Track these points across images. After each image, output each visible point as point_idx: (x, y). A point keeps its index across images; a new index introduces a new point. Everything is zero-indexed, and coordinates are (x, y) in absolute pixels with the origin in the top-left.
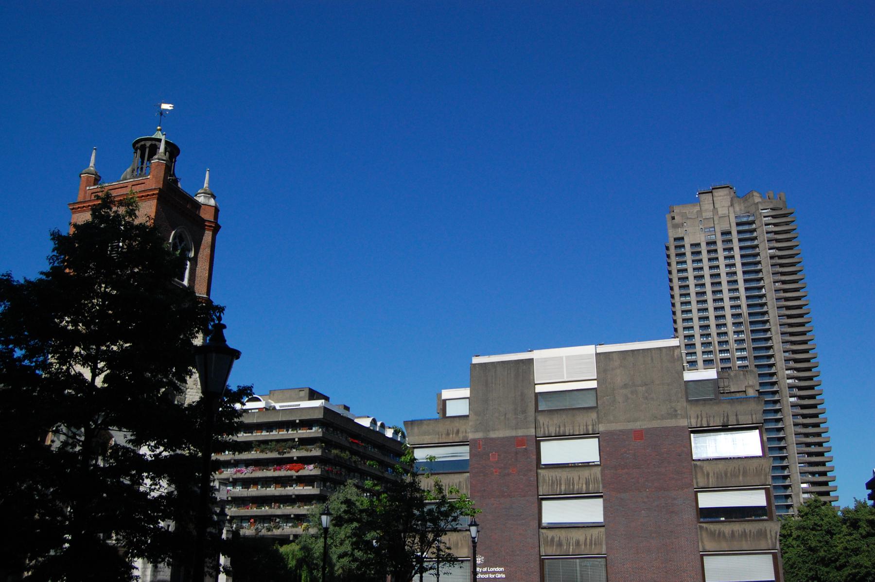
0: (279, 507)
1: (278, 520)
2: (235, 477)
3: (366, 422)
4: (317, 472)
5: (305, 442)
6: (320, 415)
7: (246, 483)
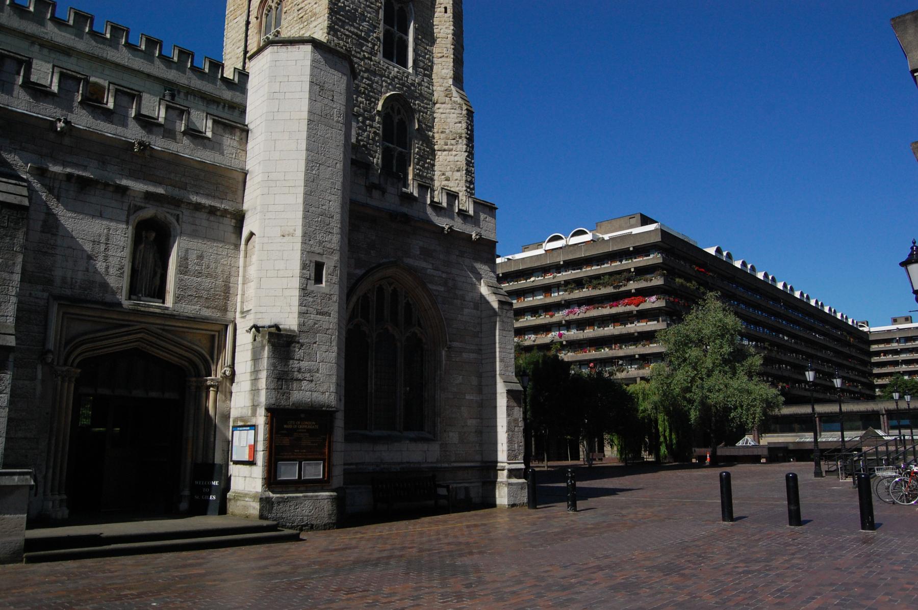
0: (621, 348)
1: (620, 362)
2: (567, 318)
3: (712, 251)
4: (661, 304)
5: (642, 272)
6: (658, 238)
7: (581, 324)
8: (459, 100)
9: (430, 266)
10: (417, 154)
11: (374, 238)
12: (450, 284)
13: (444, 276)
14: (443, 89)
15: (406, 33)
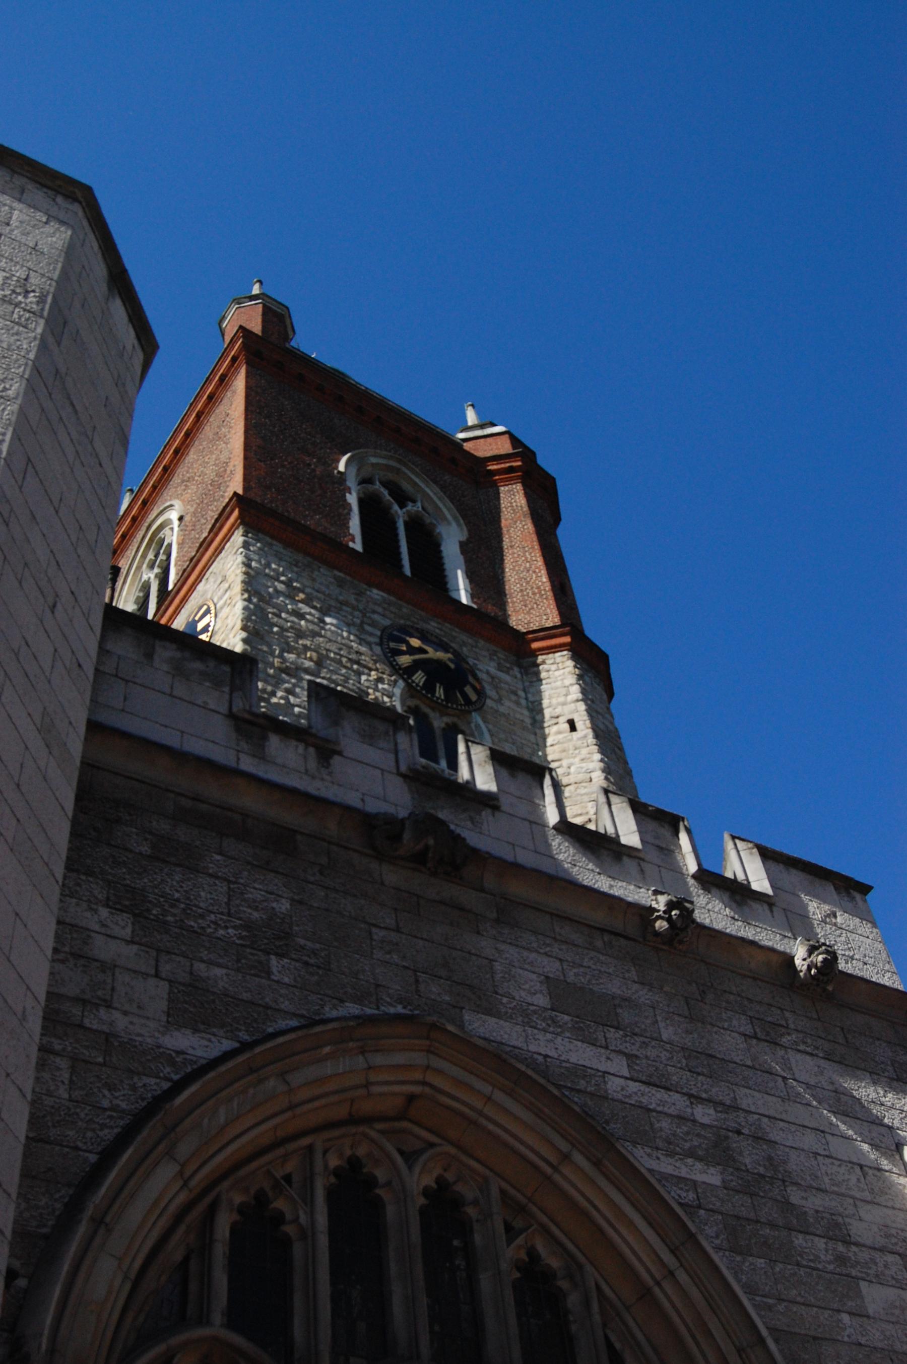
9: (619, 1065)
11: (284, 906)
12: (750, 1157)
13: (704, 1114)
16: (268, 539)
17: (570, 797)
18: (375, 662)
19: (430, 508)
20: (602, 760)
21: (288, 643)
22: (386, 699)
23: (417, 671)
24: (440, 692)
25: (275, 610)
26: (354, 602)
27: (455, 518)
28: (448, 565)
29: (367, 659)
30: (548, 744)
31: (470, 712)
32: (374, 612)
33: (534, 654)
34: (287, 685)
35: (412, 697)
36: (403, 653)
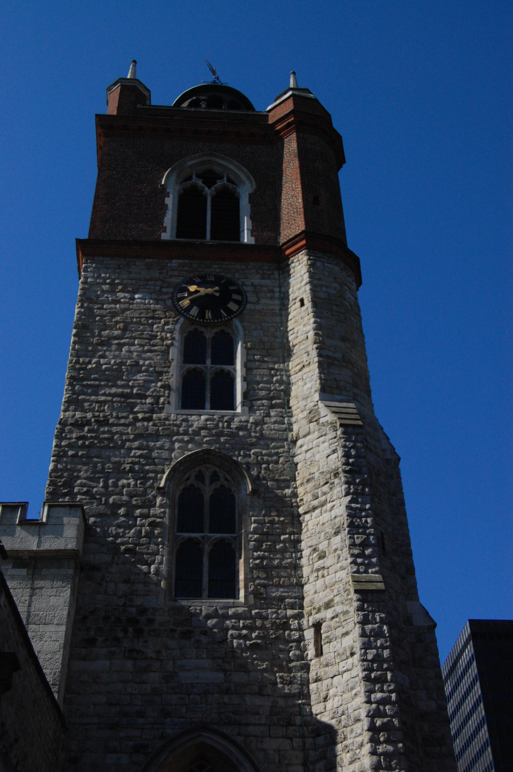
8: (330, 417)
10: (255, 532)
14: (306, 413)
15: (232, 361)
16: (101, 258)
17: (296, 353)
18: (165, 312)
19: (233, 178)
20: (315, 322)
21: (105, 324)
22: (168, 335)
23: (193, 307)
24: (208, 315)
25: (99, 306)
26: (157, 275)
27: (249, 178)
28: (241, 215)
29: (160, 312)
30: (289, 319)
31: (232, 319)
32: (171, 276)
33: (288, 258)
34: (100, 353)
35: (192, 324)
36: (184, 298)
